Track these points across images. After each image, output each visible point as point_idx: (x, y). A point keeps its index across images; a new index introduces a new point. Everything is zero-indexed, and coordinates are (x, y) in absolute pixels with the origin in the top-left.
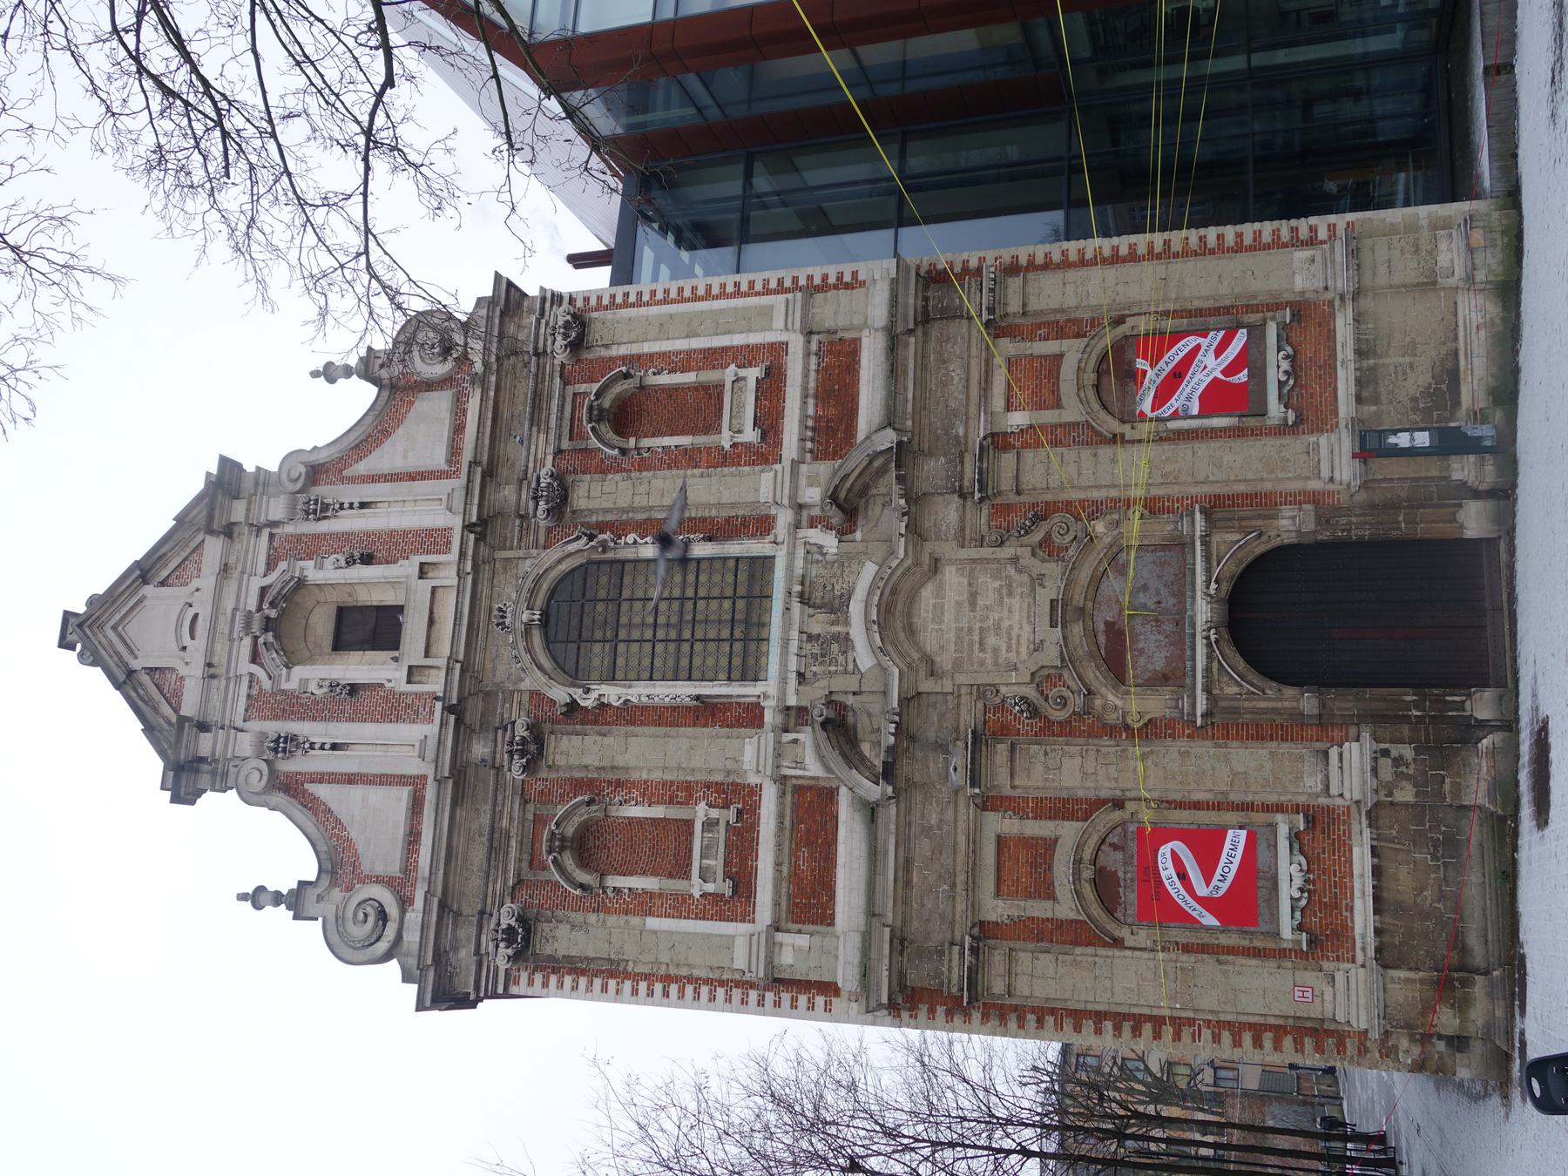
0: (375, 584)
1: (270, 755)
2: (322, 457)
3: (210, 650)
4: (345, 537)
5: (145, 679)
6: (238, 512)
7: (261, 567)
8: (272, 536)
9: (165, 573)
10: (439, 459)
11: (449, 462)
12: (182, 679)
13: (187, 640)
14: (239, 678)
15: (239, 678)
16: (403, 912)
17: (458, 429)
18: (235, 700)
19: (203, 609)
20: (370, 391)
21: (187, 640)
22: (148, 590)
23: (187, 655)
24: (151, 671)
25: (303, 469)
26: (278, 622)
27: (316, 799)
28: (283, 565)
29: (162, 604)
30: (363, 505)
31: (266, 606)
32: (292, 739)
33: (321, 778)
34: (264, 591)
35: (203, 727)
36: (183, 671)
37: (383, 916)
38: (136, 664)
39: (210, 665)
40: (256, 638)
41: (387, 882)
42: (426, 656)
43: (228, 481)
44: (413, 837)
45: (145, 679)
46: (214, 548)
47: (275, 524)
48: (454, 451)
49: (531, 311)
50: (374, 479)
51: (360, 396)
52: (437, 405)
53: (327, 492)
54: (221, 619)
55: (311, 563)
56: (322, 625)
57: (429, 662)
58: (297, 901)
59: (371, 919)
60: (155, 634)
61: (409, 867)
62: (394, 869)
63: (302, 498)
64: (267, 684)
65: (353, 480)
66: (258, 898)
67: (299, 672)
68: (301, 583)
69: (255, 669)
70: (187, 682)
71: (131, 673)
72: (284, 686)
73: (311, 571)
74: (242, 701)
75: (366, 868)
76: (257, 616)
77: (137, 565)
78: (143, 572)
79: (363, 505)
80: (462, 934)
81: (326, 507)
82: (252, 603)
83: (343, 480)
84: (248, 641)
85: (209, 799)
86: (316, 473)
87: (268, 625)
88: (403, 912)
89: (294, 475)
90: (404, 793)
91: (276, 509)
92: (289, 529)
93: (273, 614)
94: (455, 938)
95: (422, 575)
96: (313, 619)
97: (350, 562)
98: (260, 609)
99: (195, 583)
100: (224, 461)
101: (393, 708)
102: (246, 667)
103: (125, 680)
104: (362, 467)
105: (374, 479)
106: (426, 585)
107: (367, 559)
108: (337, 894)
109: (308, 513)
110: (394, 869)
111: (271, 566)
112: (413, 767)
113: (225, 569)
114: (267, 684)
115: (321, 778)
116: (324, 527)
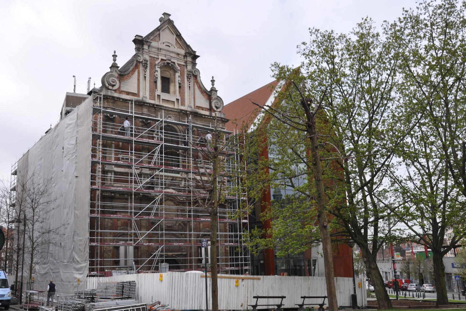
0: (174, 87)
1: (144, 62)
2: (198, 78)
3: (164, 50)
4: (184, 82)
5: (158, 33)
6: (189, 59)
7: (179, 63)
8: (184, 65)
9: (178, 40)
10: (197, 104)
11: (197, 106)
12: (158, 42)
13: (165, 44)
14: (158, 55)
15: (158, 55)
16: (114, 90)
17: (202, 109)
18: (155, 55)
19: (171, 49)
20: (209, 89)
21: (165, 44)
22: (175, 36)
23: (162, 44)
24: (159, 35)
25: (196, 74)
26: (168, 66)
27: (134, 71)
28: (179, 68)
29: (172, 38)
30: (190, 87)
31: (172, 64)
32: (146, 68)
33: (139, 73)
34: (174, 63)
35: (149, 46)
36: (159, 42)
37: (113, 86)
38: (161, 31)
39: (161, 49)
40: (165, 60)
41: (119, 87)
42: (162, 99)
43: (195, 57)
44: (128, 93)
45: (158, 33)
46: (182, 52)
47: (186, 66)
48: (199, 107)
49: (222, 126)
50: (194, 89)
51: (208, 87)
52: (206, 105)
53: (192, 79)
54: (169, 53)
55: (179, 75)
56: (167, 75)
57: (161, 100)
58: (114, 66)
59: (112, 83)
60: (167, 37)
61: (121, 92)
62: (122, 89)
63: (192, 74)
64: (157, 62)
65: (194, 85)
66: (115, 56)
67: (159, 70)
68: (175, 72)
69: (160, 60)
70: (157, 43)
71: (159, 30)
72: (157, 66)
73: (178, 74)
74: (153, 56)
75: (122, 83)
76: (170, 62)
77: (180, 35)
78: (179, 36)
79: (190, 87)
80: (111, 104)
81: (190, 79)
82: (172, 60)
83: (194, 82)
84: (165, 58)
85: (134, 46)
86: (194, 75)
87: (168, 63)
88: (114, 90)
89: (196, 72)
90: (136, 92)
91: (189, 67)
92: (185, 70)
93: (170, 65)
94: (109, 102)
95: (177, 99)
96: (167, 73)
97: (180, 84)
98: (172, 62)
99: (176, 47)
100: (198, 56)
101: (152, 91)
102: (160, 57)
103: (158, 29)
104: (196, 87)
105: (194, 89)
106: (175, 100)
107: (180, 87)
108: (117, 75)
109: (189, 74)
110: (122, 89)
111: (178, 64)
112: (141, 94)
113: (178, 54)
114: (157, 62)
115: (139, 73)
116: (186, 78)
